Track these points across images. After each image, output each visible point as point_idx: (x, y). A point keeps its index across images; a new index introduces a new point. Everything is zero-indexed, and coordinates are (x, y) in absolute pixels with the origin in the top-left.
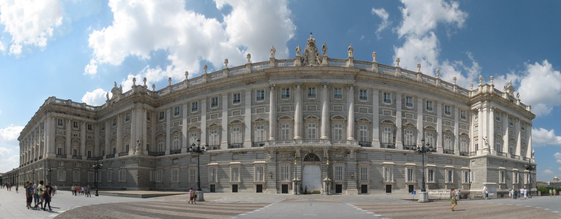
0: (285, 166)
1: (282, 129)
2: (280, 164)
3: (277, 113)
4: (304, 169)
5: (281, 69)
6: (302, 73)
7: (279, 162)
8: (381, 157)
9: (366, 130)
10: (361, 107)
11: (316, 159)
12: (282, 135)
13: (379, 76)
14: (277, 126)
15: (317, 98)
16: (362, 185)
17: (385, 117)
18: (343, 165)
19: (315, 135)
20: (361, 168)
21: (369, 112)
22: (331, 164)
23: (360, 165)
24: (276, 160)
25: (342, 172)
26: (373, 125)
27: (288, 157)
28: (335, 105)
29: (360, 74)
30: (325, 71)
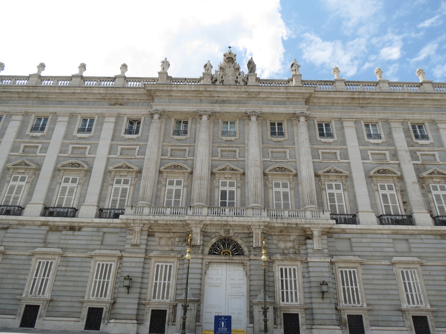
0: (164, 264)
1: (168, 187)
2: (153, 260)
3: (161, 159)
4: (208, 272)
5: (177, 87)
6: (213, 95)
7: (152, 254)
8: (385, 245)
9: (341, 191)
10: (323, 151)
11: (237, 250)
12: (165, 199)
13: (352, 96)
14: (158, 181)
15: (238, 137)
16: (348, 315)
17: (376, 165)
18: (297, 265)
19: (234, 203)
20: (342, 271)
21: (341, 159)
22: (270, 262)
23: (337, 265)
24: (146, 250)
25: (295, 281)
26: (354, 180)
27: (173, 245)
28: (273, 148)
29: (316, 97)
30: (253, 92)
